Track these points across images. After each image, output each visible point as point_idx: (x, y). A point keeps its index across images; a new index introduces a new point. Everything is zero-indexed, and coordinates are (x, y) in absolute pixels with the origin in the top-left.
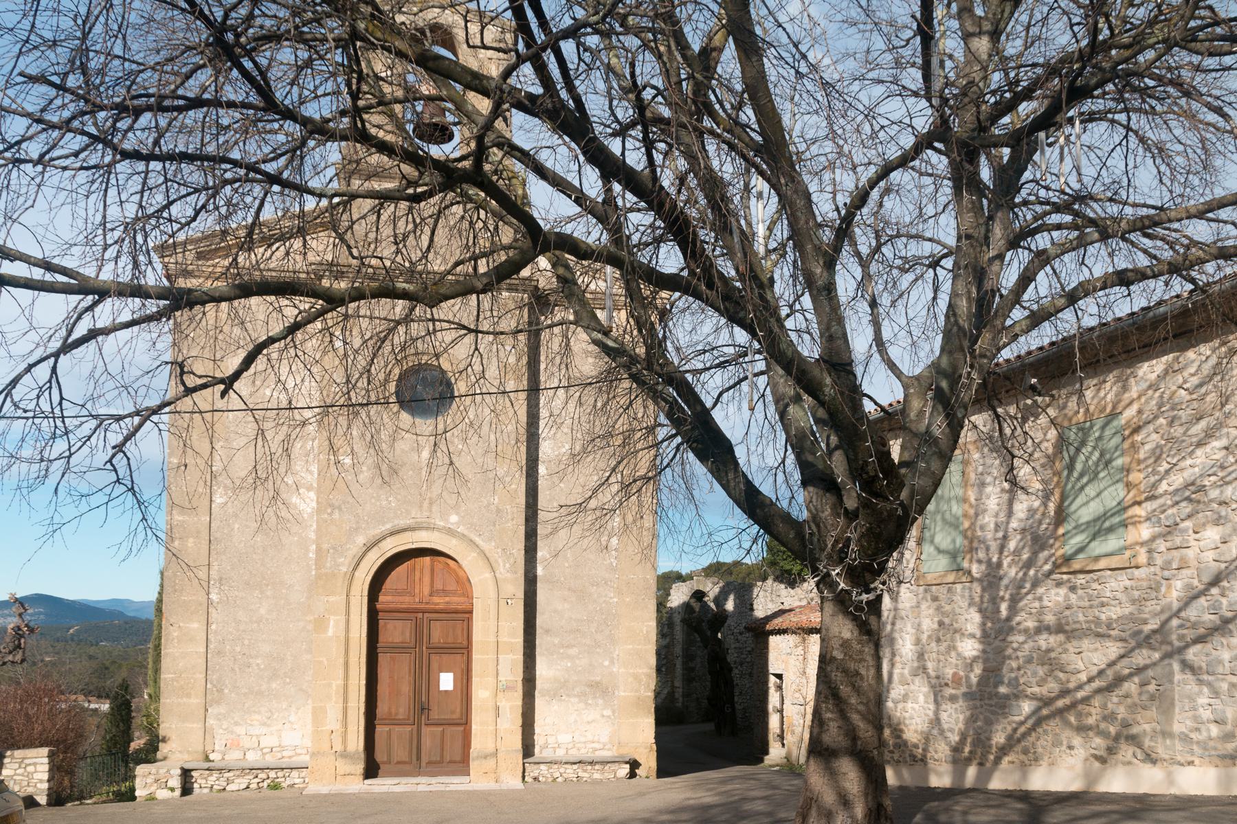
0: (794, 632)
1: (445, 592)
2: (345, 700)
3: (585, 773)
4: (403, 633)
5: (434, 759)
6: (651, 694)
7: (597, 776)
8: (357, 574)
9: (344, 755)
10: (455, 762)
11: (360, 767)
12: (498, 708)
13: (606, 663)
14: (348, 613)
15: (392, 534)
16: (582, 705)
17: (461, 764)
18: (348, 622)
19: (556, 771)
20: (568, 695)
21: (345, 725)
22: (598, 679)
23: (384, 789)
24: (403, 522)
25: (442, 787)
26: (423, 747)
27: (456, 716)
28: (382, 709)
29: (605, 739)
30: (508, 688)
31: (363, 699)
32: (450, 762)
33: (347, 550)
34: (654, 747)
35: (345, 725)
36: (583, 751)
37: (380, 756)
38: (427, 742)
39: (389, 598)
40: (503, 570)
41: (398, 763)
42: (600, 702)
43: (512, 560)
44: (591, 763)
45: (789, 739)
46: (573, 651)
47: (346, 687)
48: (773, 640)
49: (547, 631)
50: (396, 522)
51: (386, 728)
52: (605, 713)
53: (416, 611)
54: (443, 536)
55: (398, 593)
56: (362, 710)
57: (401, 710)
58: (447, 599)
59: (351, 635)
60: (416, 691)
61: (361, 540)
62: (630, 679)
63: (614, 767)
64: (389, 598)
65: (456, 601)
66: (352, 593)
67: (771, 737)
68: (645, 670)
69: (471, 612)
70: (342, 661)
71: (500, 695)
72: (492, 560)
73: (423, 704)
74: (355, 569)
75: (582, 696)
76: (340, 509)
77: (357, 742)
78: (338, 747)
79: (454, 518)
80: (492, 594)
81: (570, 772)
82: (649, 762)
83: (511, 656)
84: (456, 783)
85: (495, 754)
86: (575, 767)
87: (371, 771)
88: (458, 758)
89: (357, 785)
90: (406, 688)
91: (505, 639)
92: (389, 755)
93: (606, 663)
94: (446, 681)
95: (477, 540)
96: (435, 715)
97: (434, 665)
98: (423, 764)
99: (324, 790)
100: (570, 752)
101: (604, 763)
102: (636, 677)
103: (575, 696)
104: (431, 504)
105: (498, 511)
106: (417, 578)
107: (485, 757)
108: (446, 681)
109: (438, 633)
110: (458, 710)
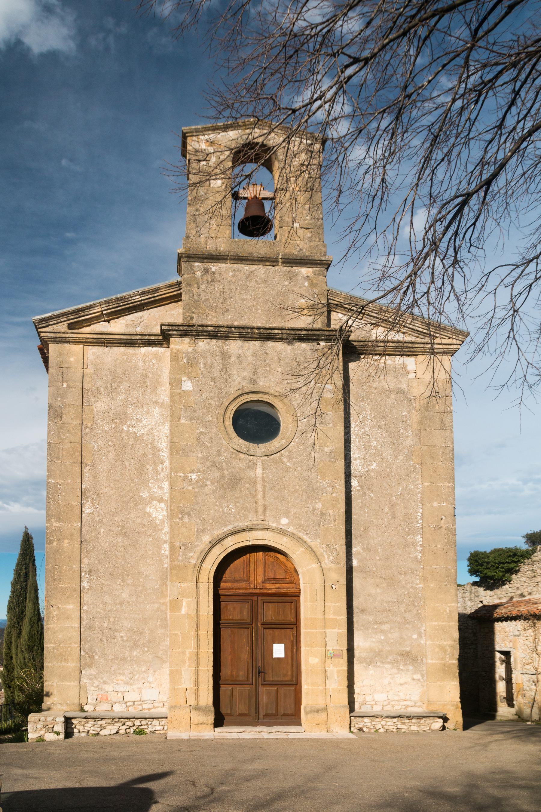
0: (525, 619)
1: (275, 580)
2: (197, 665)
3: (404, 726)
4: (241, 612)
5: (270, 712)
6: (456, 662)
7: (414, 728)
8: (204, 565)
9: (197, 708)
10: (288, 715)
11: (211, 718)
12: (326, 672)
13: (415, 637)
14: (197, 596)
15: (233, 533)
16: (395, 670)
17: (293, 717)
18: (197, 602)
19: (378, 724)
20: (382, 662)
21: (197, 684)
22: (408, 649)
23: (234, 736)
24: (241, 525)
25: (283, 736)
26: (261, 703)
27: (288, 678)
28: (225, 672)
29: (415, 698)
30: (335, 656)
31: (211, 664)
32: (284, 715)
33: (196, 546)
34: (460, 705)
35: (197, 684)
36: (396, 707)
37: (224, 710)
38: (264, 699)
39: (229, 585)
40: (328, 561)
41: (240, 715)
42: (411, 668)
43: (335, 554)
44: (408, 717)
45: (518, 700)
46: (386, 627)
47: (197, 654)
48: (498, 626)
49: (363, 611)
50: (236, 524)
51: (230, 687)
52: (415, 677)
53: (252, 595)
54: (276, 535)
55: (235, 581)
56: (211, 672)
57: (241, 673)
58: (278, 585)
59: (200, 614)
60: (253, 658)
61: (207, 539)
62: (437, 650)
63: (429, 721)
64: (229, 585)
65: (285, 588)
66: (200, 580)
67: (498, 699)
68: (450, 642)
69: (298, 596)
70: (193, 633)
71: (328, 661)
72: (318, 554)
73: (260, 668)
74: (202, 562)
75: (394, 663)
76: (189, 514)
77: (206, 698)
78: (192, 701)
79: (284, 521)
80: (318, 579)
81: (391, 724)
82: (456, 716)
83: (337, 630)
84: (291, 732)
85: (325, 709)
86: (395, 720)
87: (219, 722)
88: (290, 712)
89: (210, 733)
90: (245, 656)
91: (331, 616)
92: (232, 708)
93: (415, 637)
94: (279, 651)
95: (305, 537)
96: (270, 677)
97: (269, 638)
98: (261, 716)
99: (185, 736)
100: (385, 708)
101: (420, 717)
102: (442, 648)
103: (389, 663)
104: (265, 510)
105: (322, 514)
106: (252, 569)
107: (318, 712)
108: (279, 651)
109: (271, 612)
110: (289, 673)
